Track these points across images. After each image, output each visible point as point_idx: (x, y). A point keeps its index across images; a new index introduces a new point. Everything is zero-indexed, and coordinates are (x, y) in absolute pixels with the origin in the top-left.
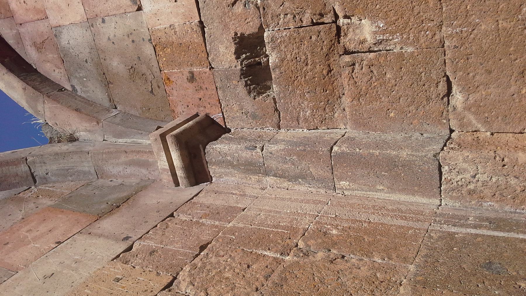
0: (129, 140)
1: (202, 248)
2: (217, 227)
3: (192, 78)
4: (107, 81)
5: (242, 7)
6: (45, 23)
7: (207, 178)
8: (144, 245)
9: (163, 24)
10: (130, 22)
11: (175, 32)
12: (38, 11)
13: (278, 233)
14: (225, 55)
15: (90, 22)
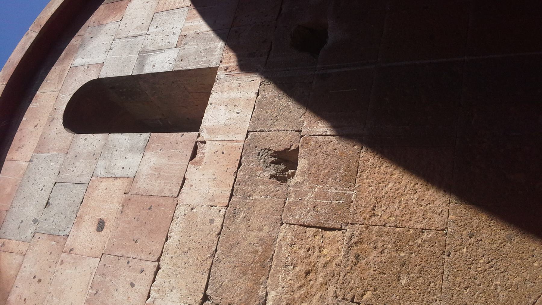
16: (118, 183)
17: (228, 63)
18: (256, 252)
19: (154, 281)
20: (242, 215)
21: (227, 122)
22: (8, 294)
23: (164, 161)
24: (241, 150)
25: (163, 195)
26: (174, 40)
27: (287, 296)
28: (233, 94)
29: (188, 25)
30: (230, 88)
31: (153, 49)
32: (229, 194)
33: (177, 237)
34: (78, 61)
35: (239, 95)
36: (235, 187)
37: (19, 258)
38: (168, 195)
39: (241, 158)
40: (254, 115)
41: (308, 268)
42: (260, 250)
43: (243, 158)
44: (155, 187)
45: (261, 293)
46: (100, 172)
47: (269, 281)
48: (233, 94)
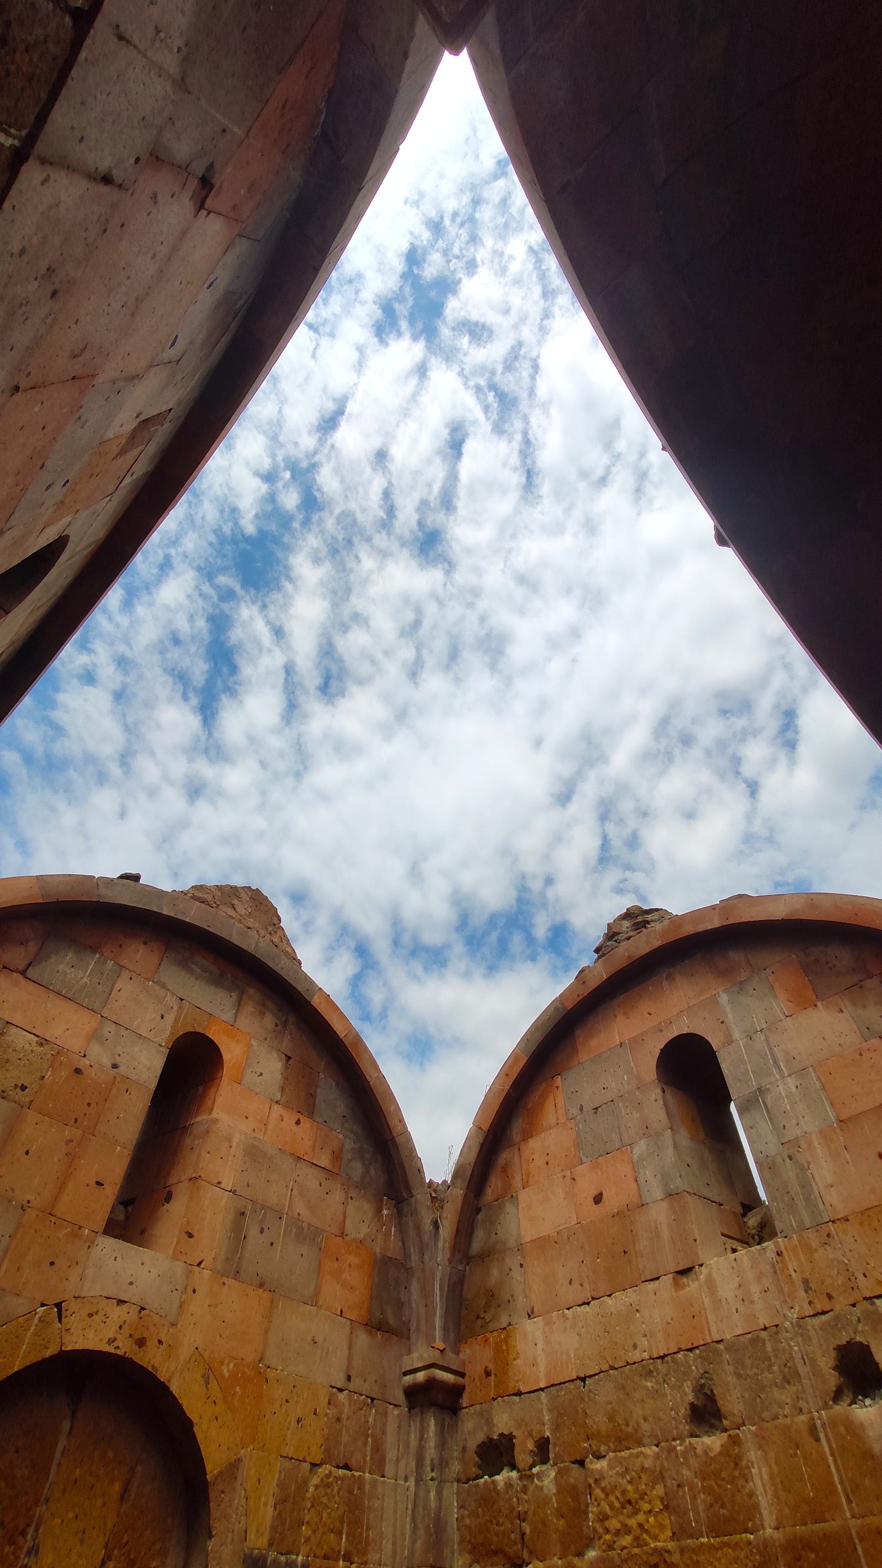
0: (438, 1299)
1: (346, 1467)
2: (365, 1461)
3: (488, 1373)
4: (486, 1256)
5: (531, 1448)
6: (520, 1185)
7: (411, 1407)
8: (343, 1404)
9: (520, 1345)
10: (521, 1300)
11: (515, 1359)
12: (528, 1174)
13: (361, 1534)
14: (503, 1421)
15: (520, 1247)
16: (633, 1185)
17: (786, 1249)
18: (627, 1425)
19: (579, 1306)
20: (649, 1384)
21: (723, 1300)
22: (531, 1137)
23: (666, 1234)
24: (702, 1343)
25: (639, 1260)
26: (790, 1135)
27: (609, 1487)
28: (755, 1289)
29: (815, 1140)
30: (759, 1278)
31: (769, 1107)
32: (662, 1354)
33: (614, 1311)
34: (724, 998)
35: (756, 1297)
36: (669, 1357)
37: (554, 1122)
38: (641, 1267)
39: (697, 1347)
40: (741, 1338)
41: (633, 1501)
42: (630, 1429)
43: (697, 1351)
44: (643, 1245)
45: (603, 1449)
46: (637, 1151)
47: (611, 1454)
48: (755, 1289)
